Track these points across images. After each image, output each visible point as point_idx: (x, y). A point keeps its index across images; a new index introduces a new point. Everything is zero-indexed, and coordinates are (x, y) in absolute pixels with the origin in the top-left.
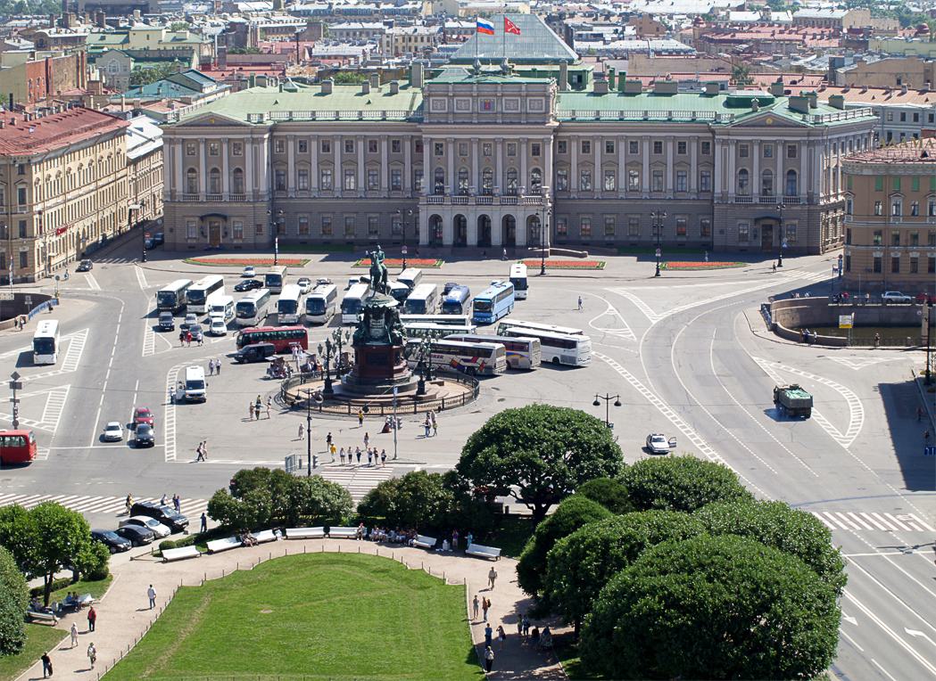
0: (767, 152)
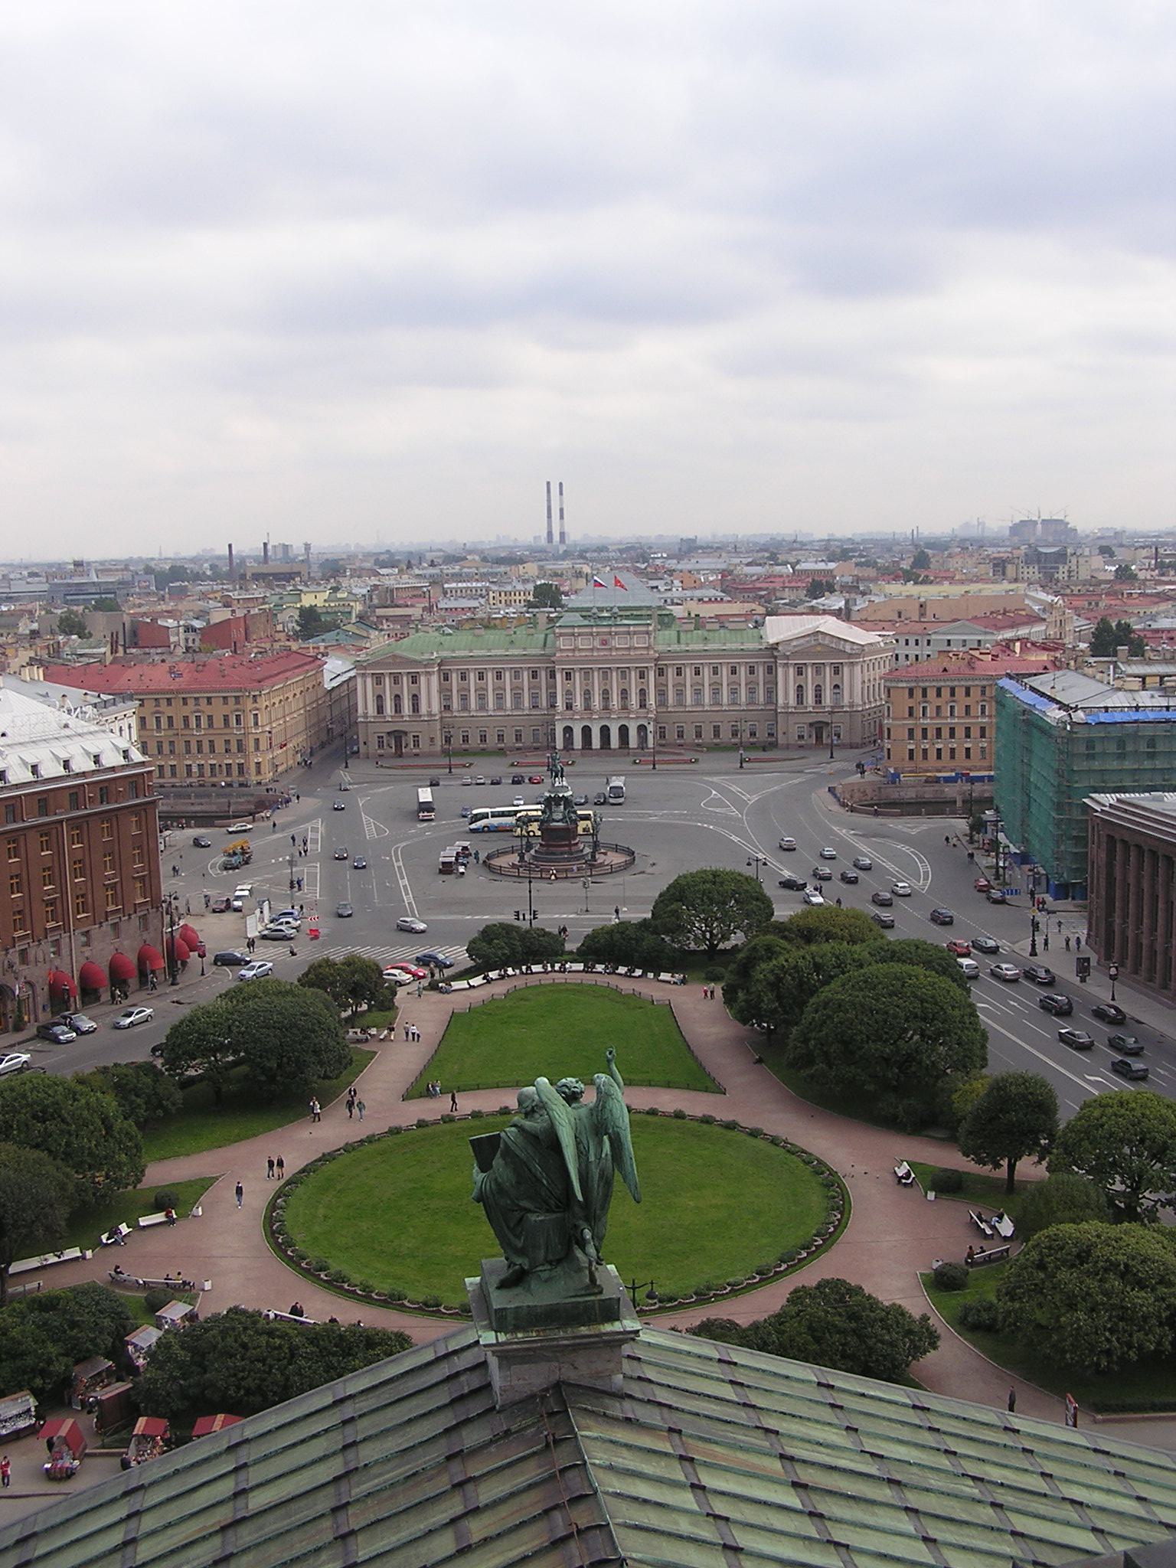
0: (818, 669)
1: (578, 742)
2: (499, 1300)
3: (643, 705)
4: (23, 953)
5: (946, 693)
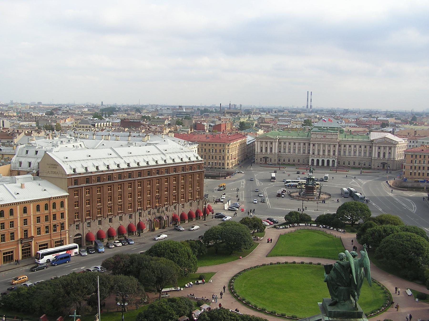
1: (315, 164)
2: (330, 309)
3: (334, 154)
4: (167, 209)
5: (422, 157)
